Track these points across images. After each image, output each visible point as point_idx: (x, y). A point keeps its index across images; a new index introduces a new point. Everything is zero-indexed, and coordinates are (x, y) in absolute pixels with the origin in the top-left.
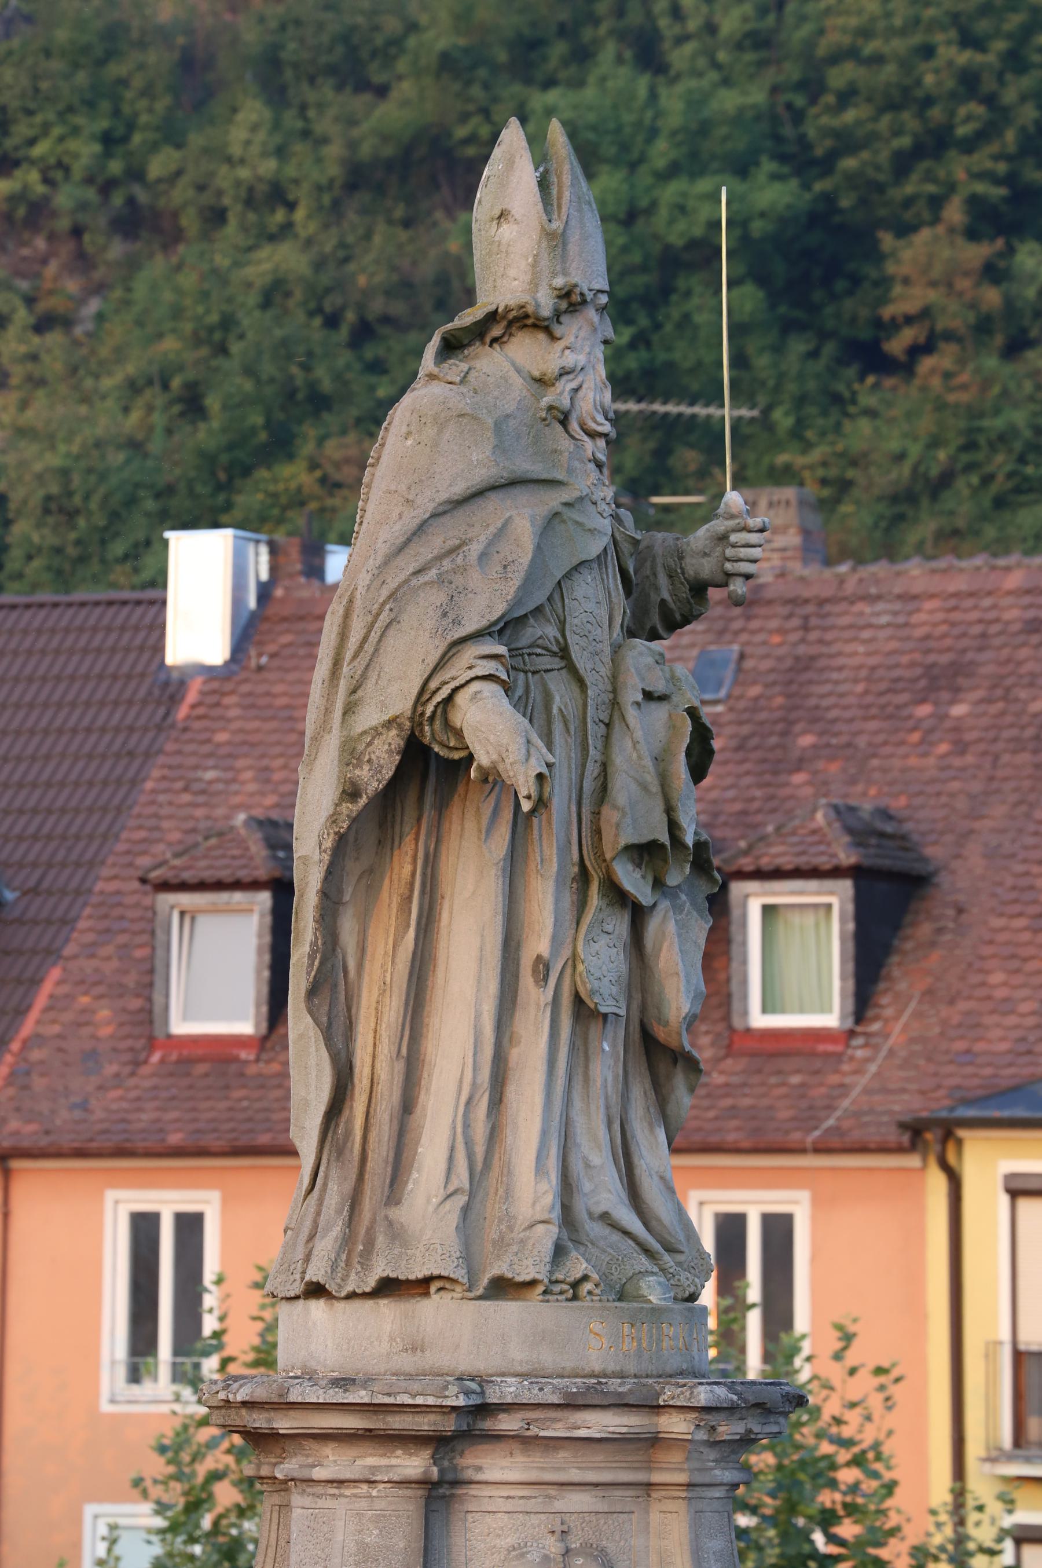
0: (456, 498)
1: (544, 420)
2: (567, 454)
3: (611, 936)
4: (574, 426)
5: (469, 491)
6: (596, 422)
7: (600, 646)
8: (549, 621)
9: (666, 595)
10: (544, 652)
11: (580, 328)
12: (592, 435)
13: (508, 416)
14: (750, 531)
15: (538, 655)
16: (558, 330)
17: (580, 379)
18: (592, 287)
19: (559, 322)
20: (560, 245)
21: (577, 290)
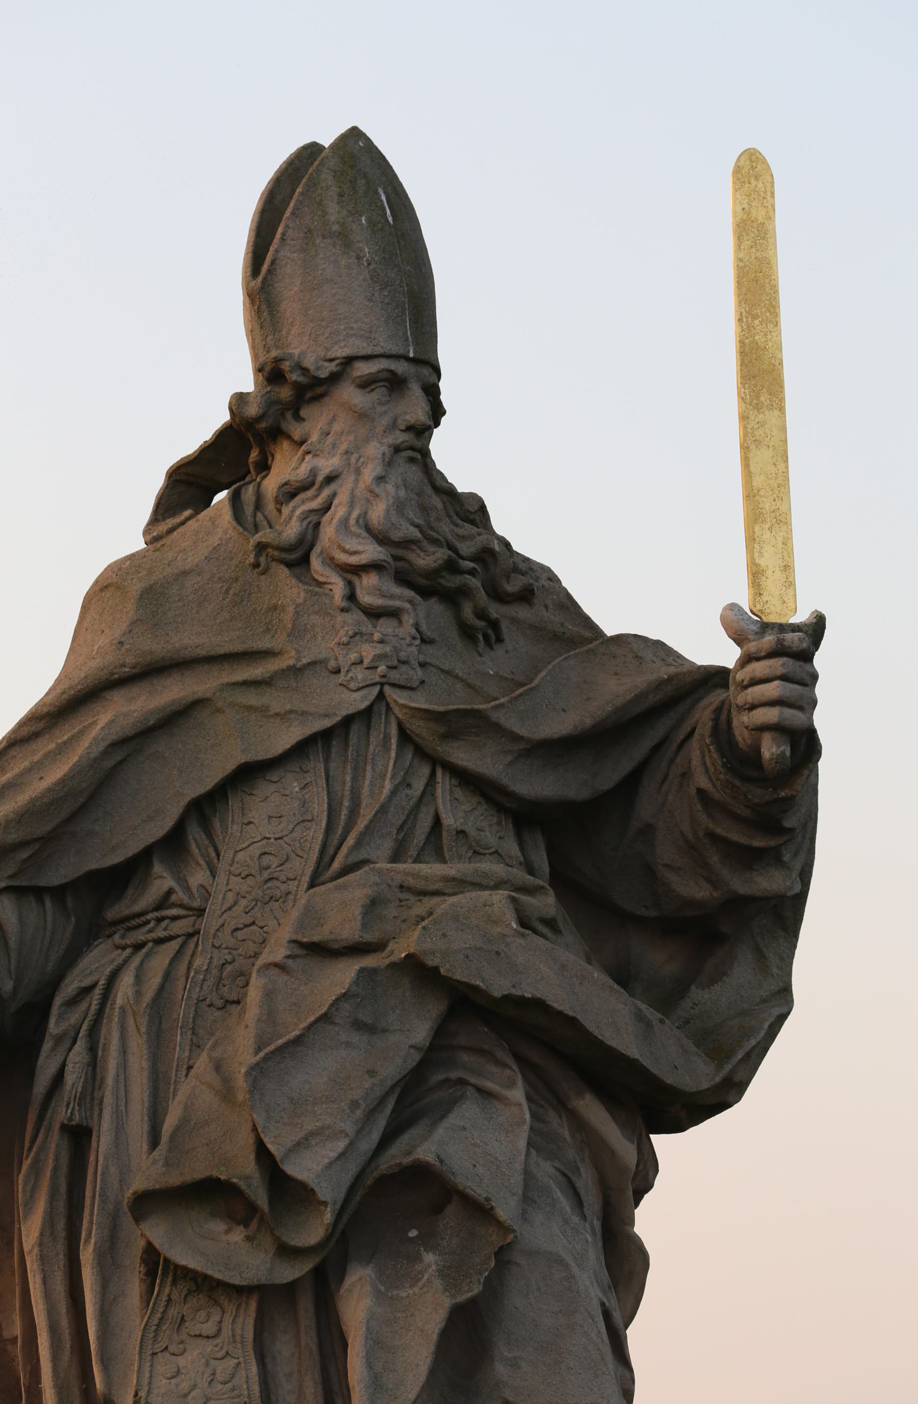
0: (45, 710)
1: (256, 565)
2: (291, 609)
3: (218, 1340)
4: (316, 563)
5: (65, 696)
6: (345, 551)
7: (292, 886)
8: (198, 863)
9: (702, 781)
10: (182, 912)
11: (334, 419)
12: (352, 571)
13: (185, 573)
14: (758, 659)
15: (175, 918)
16: (297, 431)
17: (326, 492)
18: (330, 355)
19: (298, 418)
20: (264, 307)
21: (286, 366)
